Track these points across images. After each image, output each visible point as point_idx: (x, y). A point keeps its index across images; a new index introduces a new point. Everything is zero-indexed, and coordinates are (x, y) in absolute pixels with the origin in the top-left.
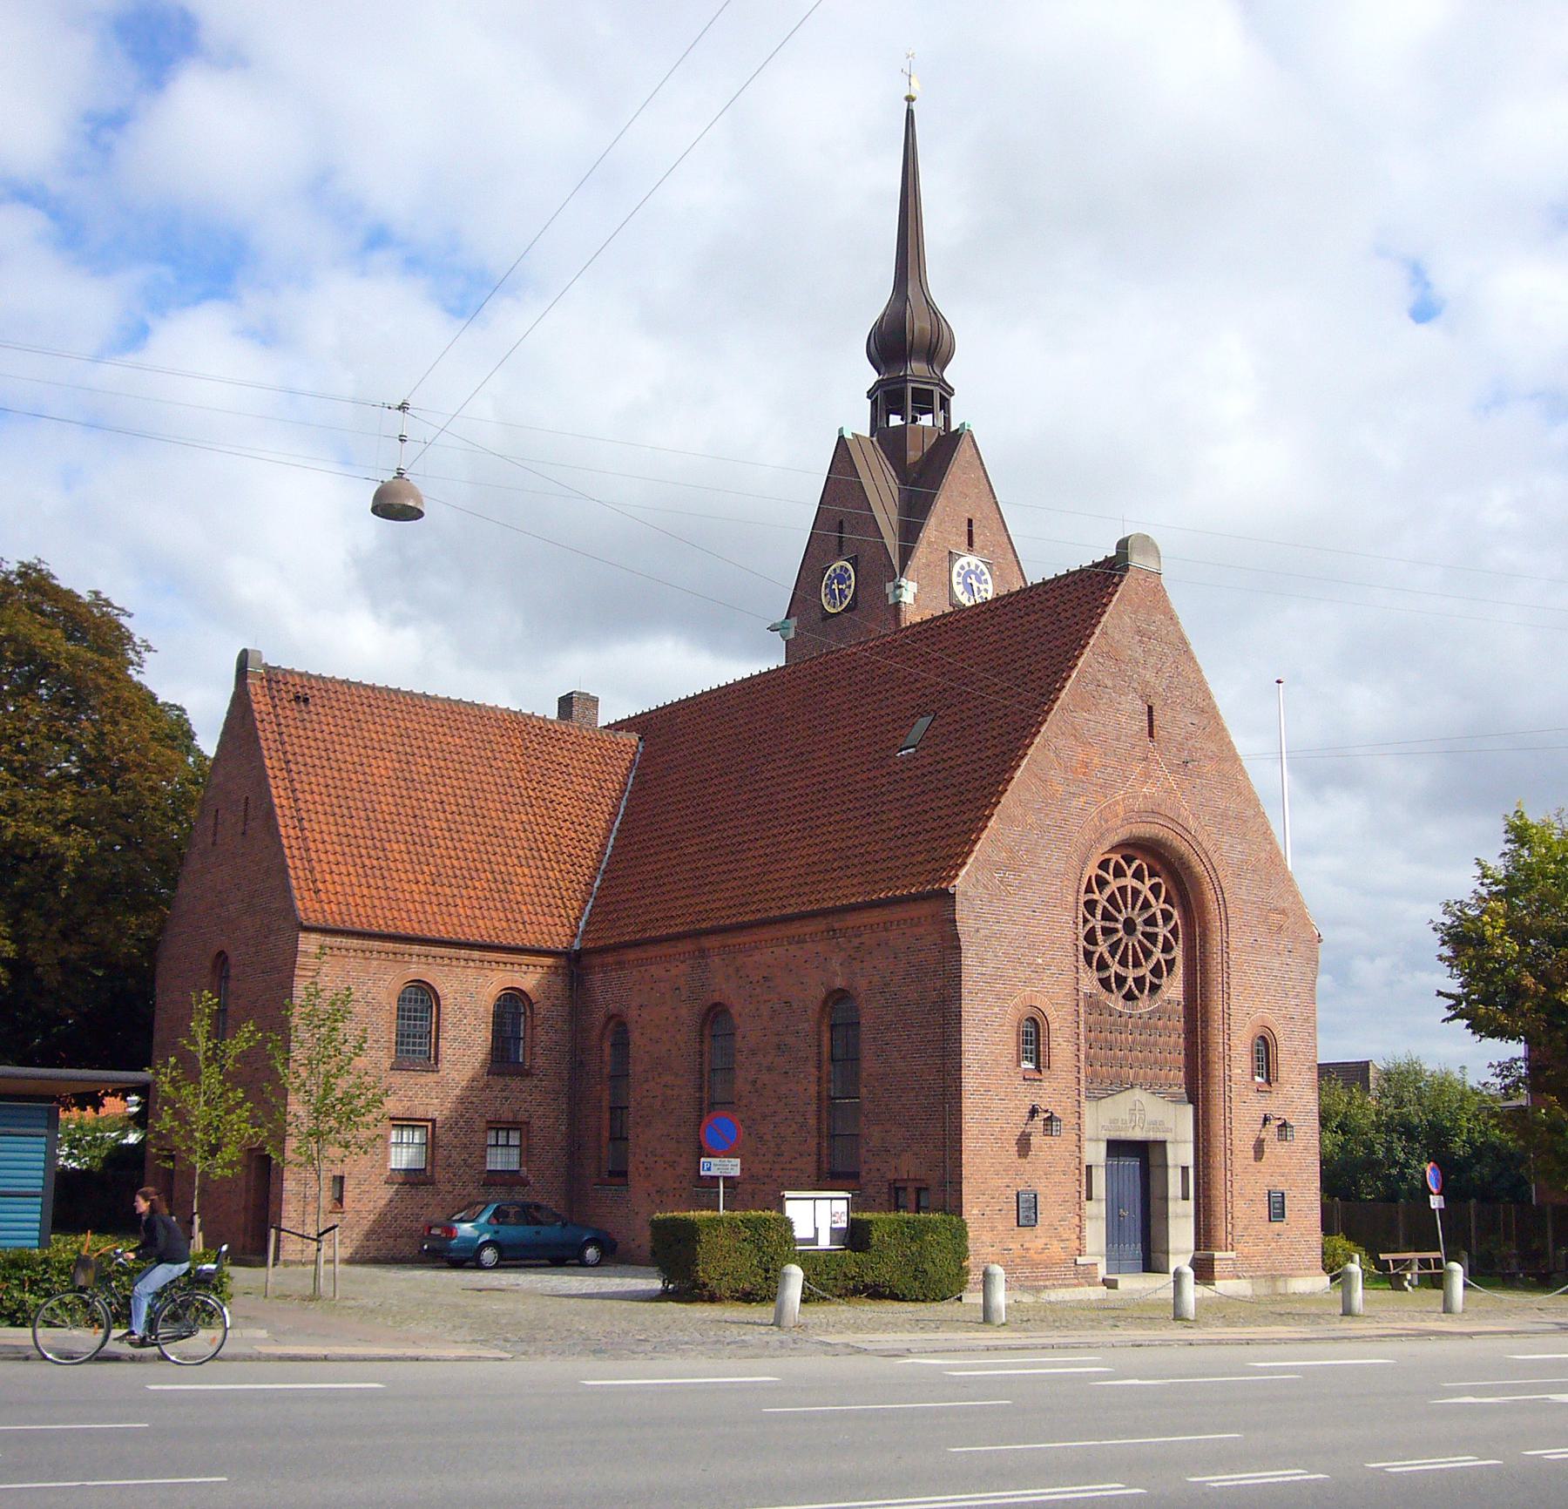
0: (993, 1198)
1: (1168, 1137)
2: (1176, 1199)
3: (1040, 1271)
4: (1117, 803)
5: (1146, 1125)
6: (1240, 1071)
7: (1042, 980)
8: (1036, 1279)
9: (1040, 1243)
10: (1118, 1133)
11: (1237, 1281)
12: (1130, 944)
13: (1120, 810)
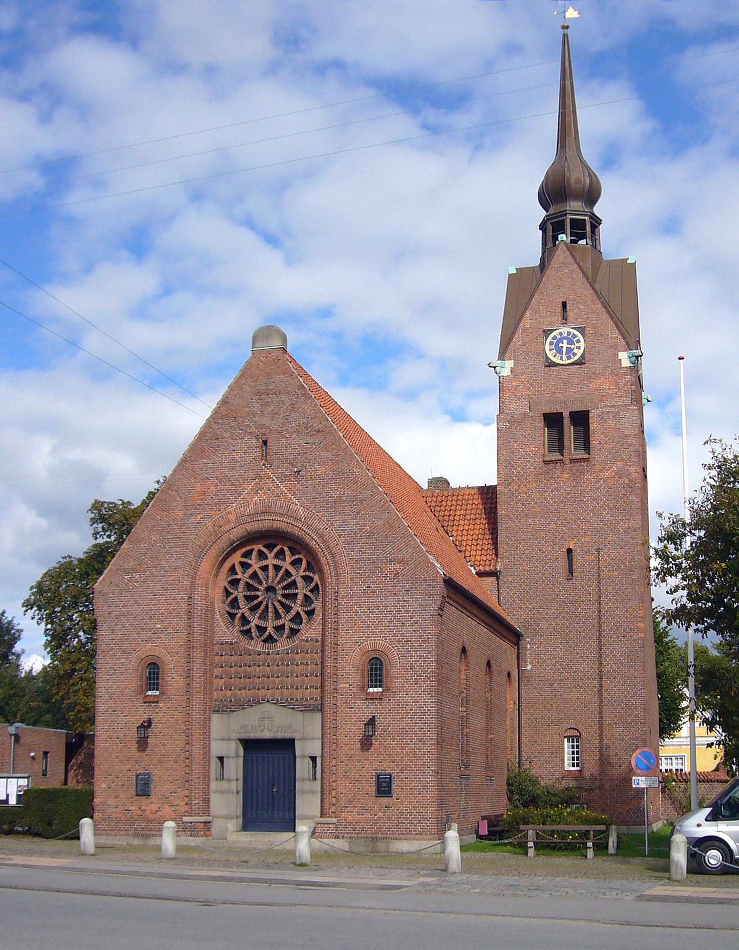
0: (118, 778)
1: (296, 736)
2: (303, 780)
3: (151, 826)
4: (230, 513)
7: (161, 638)
8: (151, 830)
9: (154, 807)
10: (248, 735)
13: (232, 517)
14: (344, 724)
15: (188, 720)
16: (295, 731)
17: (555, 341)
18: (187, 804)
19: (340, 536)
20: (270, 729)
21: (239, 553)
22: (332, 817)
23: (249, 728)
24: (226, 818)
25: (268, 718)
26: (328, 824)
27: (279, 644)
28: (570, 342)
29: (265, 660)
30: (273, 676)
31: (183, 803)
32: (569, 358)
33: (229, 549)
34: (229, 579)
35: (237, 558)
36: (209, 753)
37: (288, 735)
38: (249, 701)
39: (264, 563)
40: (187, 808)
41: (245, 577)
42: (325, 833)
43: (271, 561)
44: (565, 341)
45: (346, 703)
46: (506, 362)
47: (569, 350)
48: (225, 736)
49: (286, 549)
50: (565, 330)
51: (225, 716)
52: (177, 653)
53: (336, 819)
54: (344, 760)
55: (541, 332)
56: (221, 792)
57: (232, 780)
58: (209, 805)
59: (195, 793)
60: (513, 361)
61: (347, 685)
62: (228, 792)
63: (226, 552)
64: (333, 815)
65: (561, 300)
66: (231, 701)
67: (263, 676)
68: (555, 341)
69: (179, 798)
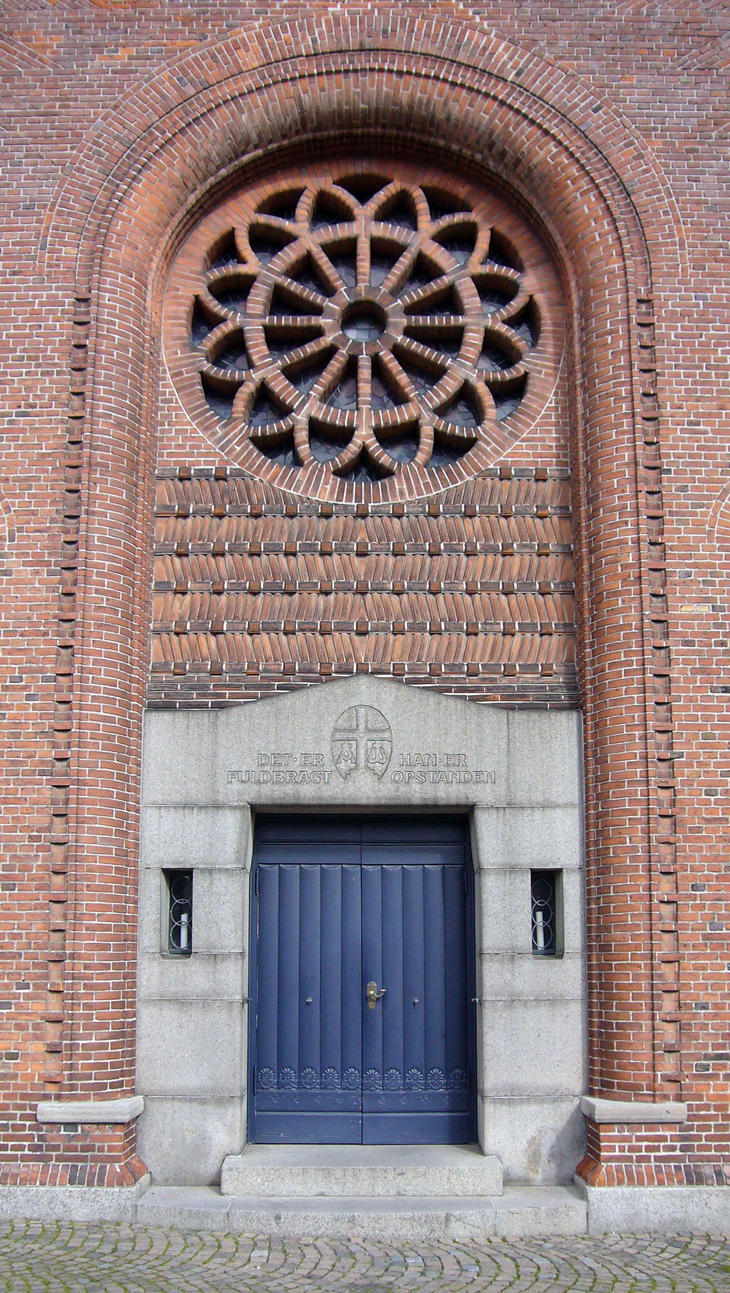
1: (480, 794)
2: (513, 955)
5: (394, 767)
10: (290, 789)
11: (686, 1189)
12: (387, 357)
16: (478, 777)
18: (54, 1051)
19: (647, 132)
20: (379, 767)
22: (666, 1098)
24: (203, 1102)
25: (368, 730)
27: (398, 483)
29: (346, 535)
30: (380, 590)
31: (41, 1047)
33: (223, 172)
34: (216, 274)
36: (137, 855)
38: (288, 671)
39: (341, 231)
40: (52, 1066)
41: (270, 270)
42: (640, 1159)
49: (418, 194)
51: (205, 718)
53: (683, 1106)
54: (708, 878)
56: (181, 1002)
57: (225, 957)
58: (133, 1053)
59: (88, 1006)
61: (705, 609)
62: (206, 1001)
63: (212, 180)
66: (216, 672)
67: (345, 588)
69: (19, 1027)
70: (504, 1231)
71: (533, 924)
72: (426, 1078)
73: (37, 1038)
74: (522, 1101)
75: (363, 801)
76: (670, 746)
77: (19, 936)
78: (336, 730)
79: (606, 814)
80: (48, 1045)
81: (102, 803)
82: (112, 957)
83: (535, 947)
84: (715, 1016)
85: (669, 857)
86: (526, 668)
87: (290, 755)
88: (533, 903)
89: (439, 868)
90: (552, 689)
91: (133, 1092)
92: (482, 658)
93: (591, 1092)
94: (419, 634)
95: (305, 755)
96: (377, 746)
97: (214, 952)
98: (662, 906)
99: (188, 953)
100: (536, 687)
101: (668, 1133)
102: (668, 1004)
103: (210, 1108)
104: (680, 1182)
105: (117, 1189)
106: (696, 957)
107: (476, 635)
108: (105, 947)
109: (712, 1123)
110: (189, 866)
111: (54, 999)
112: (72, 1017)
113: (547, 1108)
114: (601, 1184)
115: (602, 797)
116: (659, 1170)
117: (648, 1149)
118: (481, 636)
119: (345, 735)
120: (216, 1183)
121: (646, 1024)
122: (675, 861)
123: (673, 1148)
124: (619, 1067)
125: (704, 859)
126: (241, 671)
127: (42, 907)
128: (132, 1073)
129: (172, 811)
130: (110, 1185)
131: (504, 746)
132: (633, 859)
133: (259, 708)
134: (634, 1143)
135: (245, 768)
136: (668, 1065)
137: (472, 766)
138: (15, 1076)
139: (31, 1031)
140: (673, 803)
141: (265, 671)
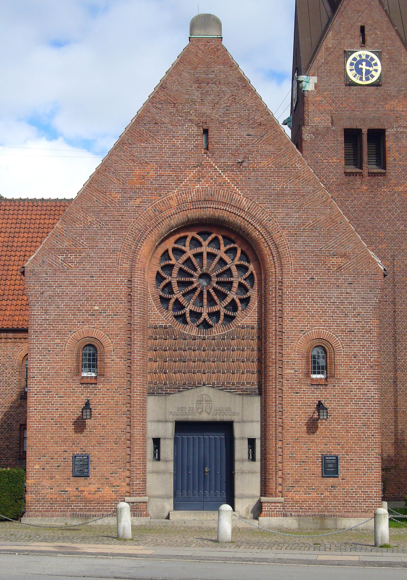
0: (53, 459)
1: (235, 418)
2: (243, 461)
3: (90, 506)
5: (212, 411)
6: (293, 371)
7: (99, 320)
8: (90, 510)
9: (93, 488)
10: (185, 417)
11: (283, 518)
12: (211, 291)
13: (173, 203)
14: (290, 408)
15: (129, 401)
16: (234, 414)
17: (355, 62)
18: (128, 485)
21: (173, 239)
22: (279, 496)
23: (187, 411)
24: (163, 498)
25: (206, 401)
26: (275, 503)
27: (214, 330)
28: (369, 64)
29: (200, 345)
30: (209, 361)
32: (367, 79)
35: (170, 244)
37: (226, 418)
38: (185, 384)
39: (199, 250)
40: (127, 488)
42: (272, 511)
43: (205, 249)
44: (364, 63)
45: (291, 388)
46: (310, 77)
47: (368, 72)
48: (161, 417)
49: (220, 237)
50: (364, 53)
52: (117, 335)
53: (283, 498)
54: (291, 442)
55: (342, 52)
56: (157, 472)
57: (169, 461)
59: (136, 474)
60: (316, 77)
62: (164, 472)
64: (280, 494)
65: (360, 24)
66: (165, 384)
67: (199, 360)
68: (355, 62)
69: (119, 479)
70: (238, 526)
71: (248, 452)
72: (220, 493)
73: (124, 481)
74: (245, 498)
75: (205, 420)
76: (282, 408)
77: (119, 456)
78: (197, 401)
79: (266, 425)
80: (127, 483)
81: (139, 422)
82: (142, 461)
83: (249, 458)
84: (292, 476)
85: (281, 436)
86: (248, 383)
87: (186, 408)
88: (248, 447)
89: (224, 437)
90: (254, 389)
91: (146, 496)
92: (236, 380)
93: (261, 496)
94: (219, 374)
95: (190, 408)
96: (208, 405)
97: (166, 460)
98: (279, 449)
99: (159, 459)
100: (250, 389)
101: (279, 505)
102: (280, 473)
103: (165, 500)
104: (281, 516)
105: (145, 518)
106: (287, 462)
107: (234, 374)
108: (140, 459)
109: (290, 503)
110: (159, 437)
111: (128, 472)
112: (133, 476)
113: (251, 500)
114: (262, 517)
115: (265, 420)
116: (277, 513)
117: (274, 509)
118: (236, 374)
119: (200, 402)
120: (168, 518)
121: (274, 478)
122: (282, 438)
123: (280, 509)
124: (268, 489)
125: (290, 437)
126: (172, 384)
127: (125, 449)
128: (145, 491)
129: (155, 422)
130: (143, 517)
131: (241, 405)
132: (272, 437)
133: (178, 395)
134: (271, 507)
135: (174, 411)
136: (280, 488)
137: (233, 411)
138: (119, 491)
139: (122, 480)
140: (282, 423)
141: (178, 384)
